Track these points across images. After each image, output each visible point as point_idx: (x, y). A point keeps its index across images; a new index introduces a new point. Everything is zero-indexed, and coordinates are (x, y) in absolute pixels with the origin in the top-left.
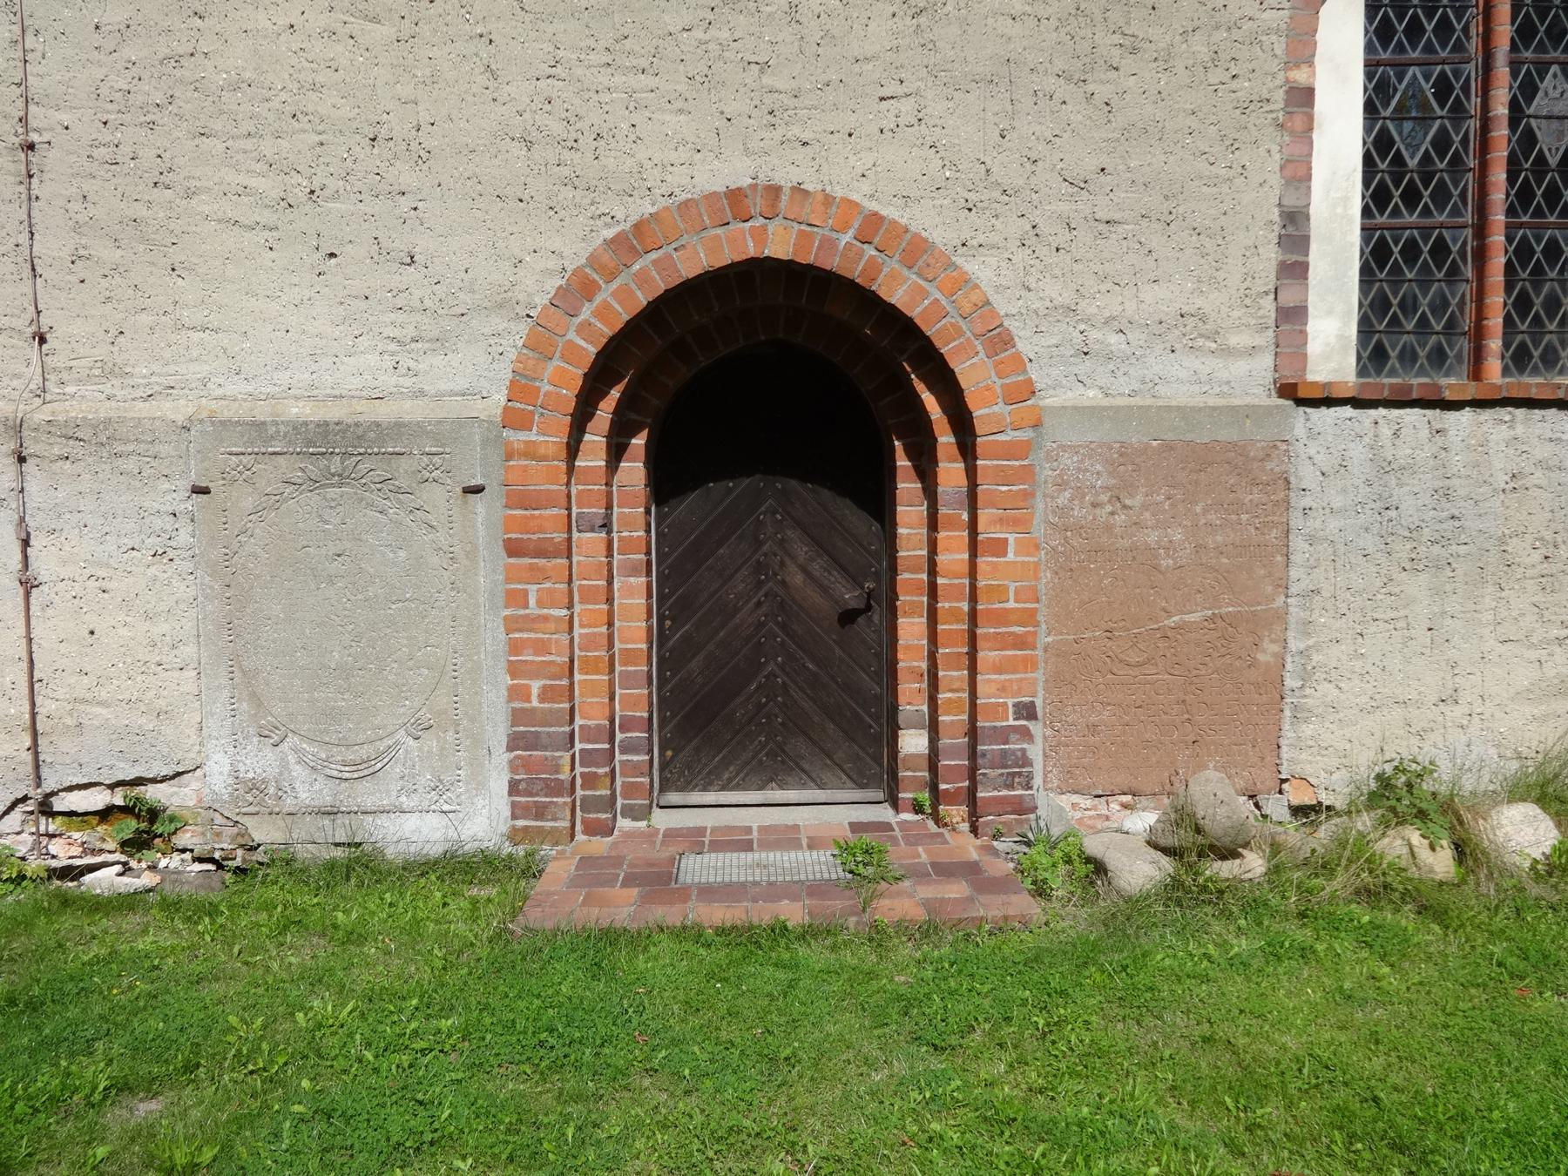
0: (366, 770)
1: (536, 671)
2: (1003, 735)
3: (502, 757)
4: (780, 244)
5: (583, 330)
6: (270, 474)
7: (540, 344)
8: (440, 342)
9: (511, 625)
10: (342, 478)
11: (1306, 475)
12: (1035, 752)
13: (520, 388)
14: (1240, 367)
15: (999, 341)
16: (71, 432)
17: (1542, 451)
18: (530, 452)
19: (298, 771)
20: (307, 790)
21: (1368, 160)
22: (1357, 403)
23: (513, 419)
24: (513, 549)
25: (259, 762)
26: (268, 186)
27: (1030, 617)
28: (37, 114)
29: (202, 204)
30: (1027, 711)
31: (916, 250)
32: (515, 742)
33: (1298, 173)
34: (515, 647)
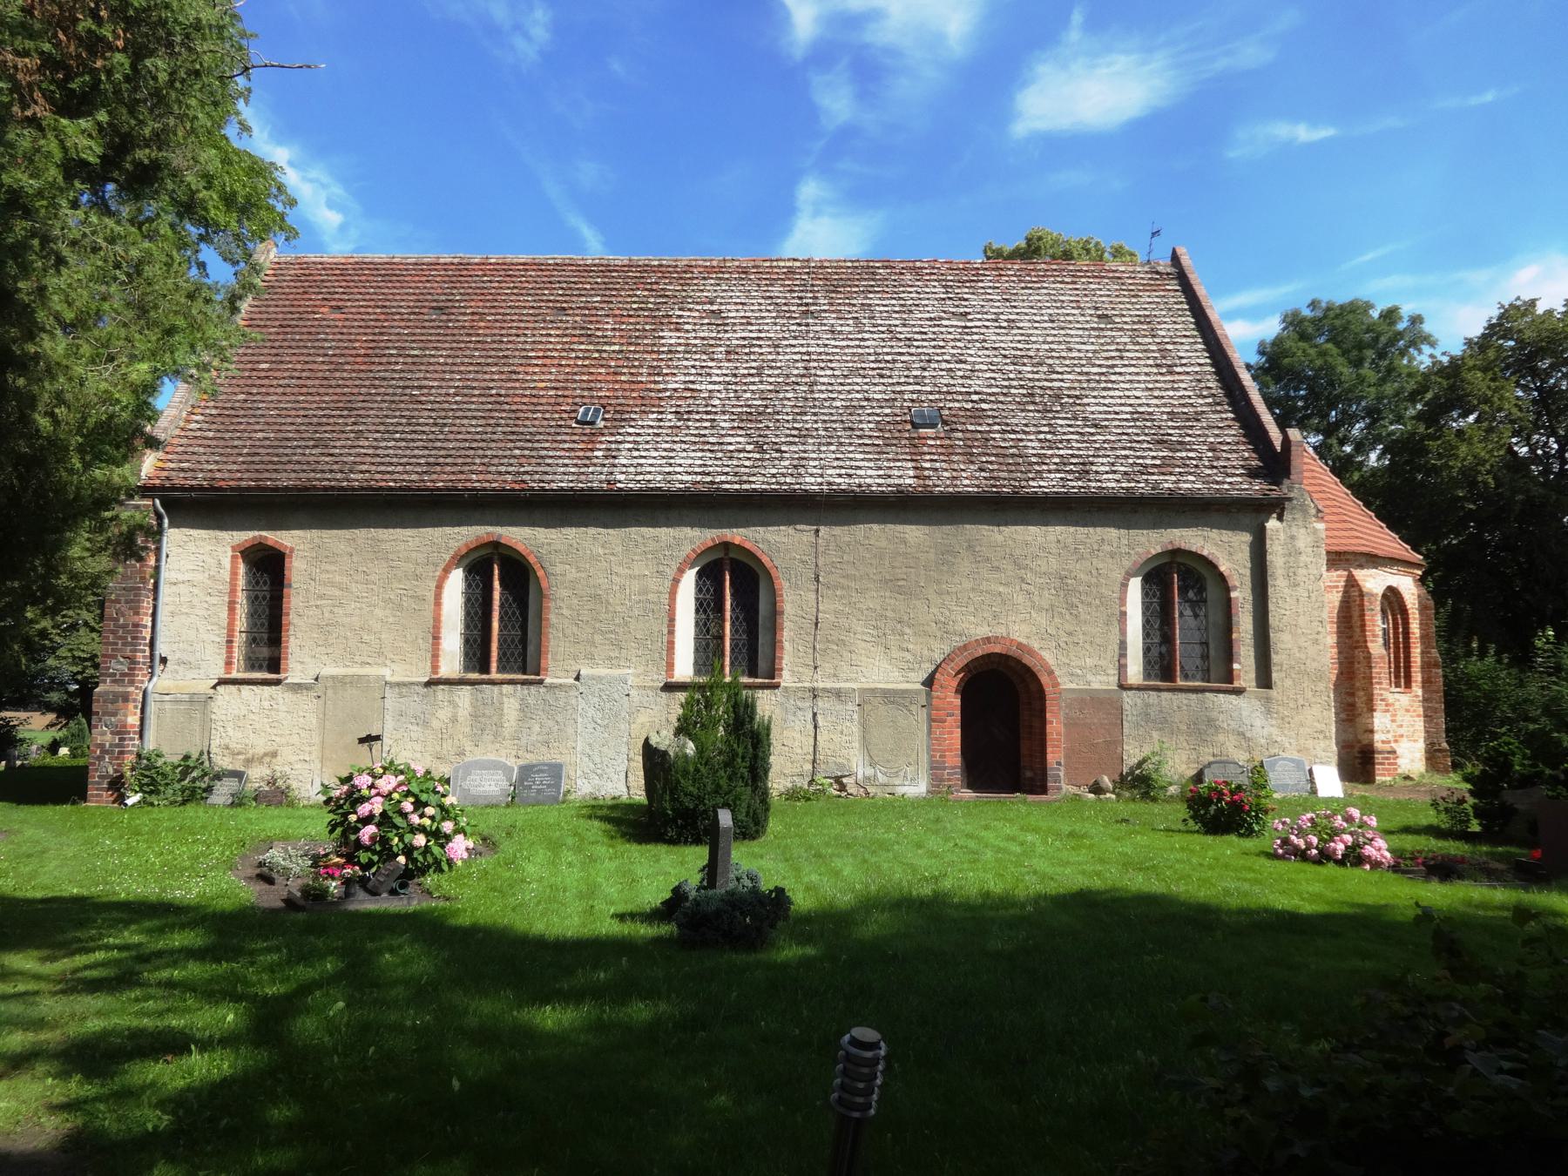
0: (896, 774)
2: (1053, 769)
4: (997, 649)
6: (875, 702)
11: (1126, 707)
12: (1062, 774)
15: (1051, 673)
17: (1185, 702)
19: (879, 775)
20: (881, 778)
21: (1144, 626)
22: (1139, 688)
25: (870, 772)
26: (875, 633)
27: (1059, 740)
30: (1059, 764)
31: (1031, 652)
32: (932, 768)
33: (1123, 632)
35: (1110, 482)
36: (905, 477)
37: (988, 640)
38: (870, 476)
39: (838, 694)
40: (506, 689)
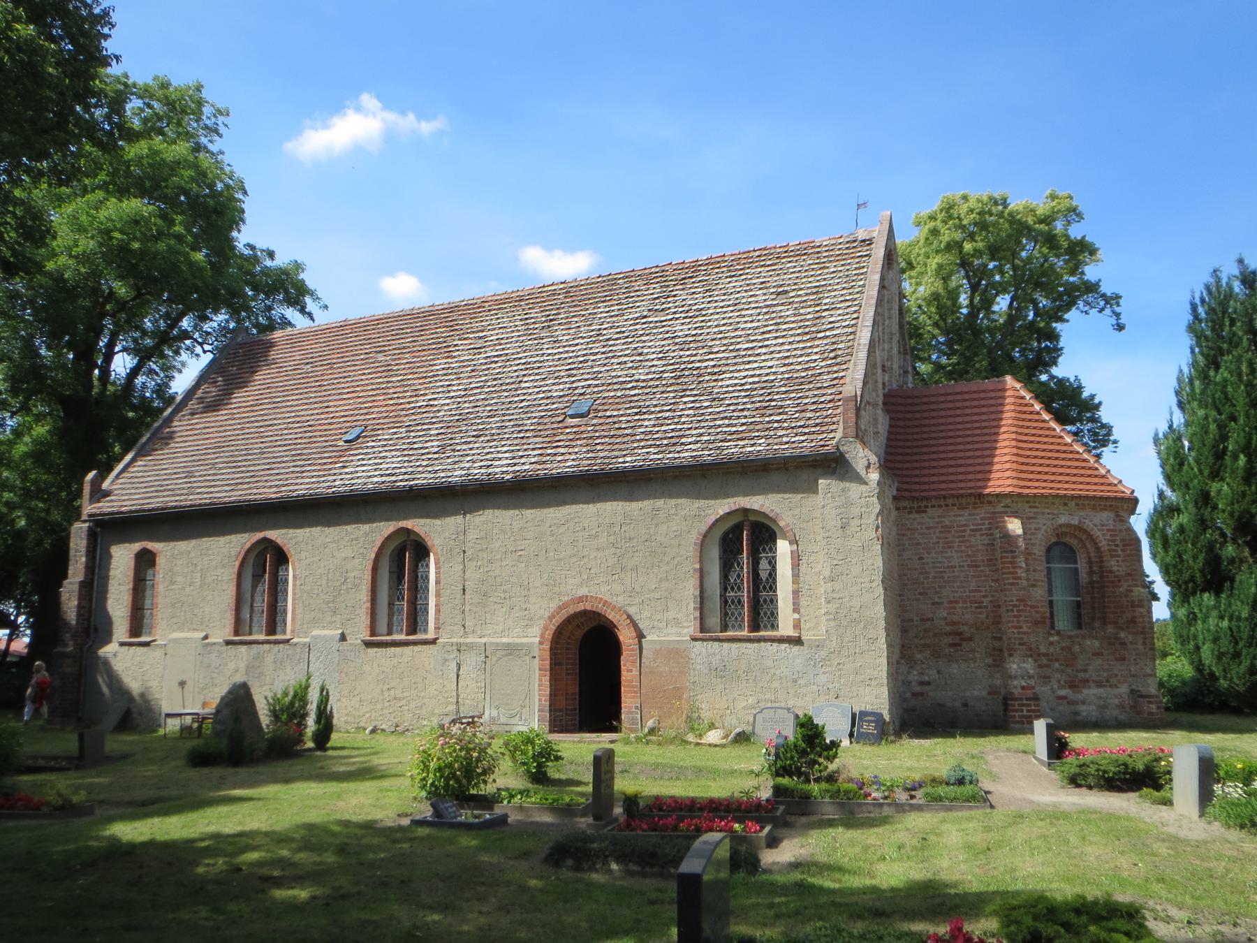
1: (543, 695)
3: (537, 714)
5: (554, 625)
7: (546, 628)
8: (532, 626)
9: (539, 686)
10: (510, 654)
11: (693, 656)
13: (542, 636)
14: (686, 630)
16: (466, 645)
18: (543, 650)
23: (541, 643)
24: (540, 670)
25: (495, 713)
26: (502, 595)
28: (467, 583)
29: (491, 599)
34: (540, 690)
35: (685, 455)
36: (528, 466)
37: (581, 599)
38: (503, 467)
39: (471, 647)
40: (266, 647)
